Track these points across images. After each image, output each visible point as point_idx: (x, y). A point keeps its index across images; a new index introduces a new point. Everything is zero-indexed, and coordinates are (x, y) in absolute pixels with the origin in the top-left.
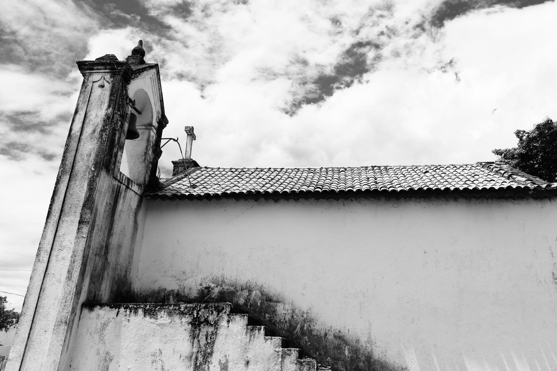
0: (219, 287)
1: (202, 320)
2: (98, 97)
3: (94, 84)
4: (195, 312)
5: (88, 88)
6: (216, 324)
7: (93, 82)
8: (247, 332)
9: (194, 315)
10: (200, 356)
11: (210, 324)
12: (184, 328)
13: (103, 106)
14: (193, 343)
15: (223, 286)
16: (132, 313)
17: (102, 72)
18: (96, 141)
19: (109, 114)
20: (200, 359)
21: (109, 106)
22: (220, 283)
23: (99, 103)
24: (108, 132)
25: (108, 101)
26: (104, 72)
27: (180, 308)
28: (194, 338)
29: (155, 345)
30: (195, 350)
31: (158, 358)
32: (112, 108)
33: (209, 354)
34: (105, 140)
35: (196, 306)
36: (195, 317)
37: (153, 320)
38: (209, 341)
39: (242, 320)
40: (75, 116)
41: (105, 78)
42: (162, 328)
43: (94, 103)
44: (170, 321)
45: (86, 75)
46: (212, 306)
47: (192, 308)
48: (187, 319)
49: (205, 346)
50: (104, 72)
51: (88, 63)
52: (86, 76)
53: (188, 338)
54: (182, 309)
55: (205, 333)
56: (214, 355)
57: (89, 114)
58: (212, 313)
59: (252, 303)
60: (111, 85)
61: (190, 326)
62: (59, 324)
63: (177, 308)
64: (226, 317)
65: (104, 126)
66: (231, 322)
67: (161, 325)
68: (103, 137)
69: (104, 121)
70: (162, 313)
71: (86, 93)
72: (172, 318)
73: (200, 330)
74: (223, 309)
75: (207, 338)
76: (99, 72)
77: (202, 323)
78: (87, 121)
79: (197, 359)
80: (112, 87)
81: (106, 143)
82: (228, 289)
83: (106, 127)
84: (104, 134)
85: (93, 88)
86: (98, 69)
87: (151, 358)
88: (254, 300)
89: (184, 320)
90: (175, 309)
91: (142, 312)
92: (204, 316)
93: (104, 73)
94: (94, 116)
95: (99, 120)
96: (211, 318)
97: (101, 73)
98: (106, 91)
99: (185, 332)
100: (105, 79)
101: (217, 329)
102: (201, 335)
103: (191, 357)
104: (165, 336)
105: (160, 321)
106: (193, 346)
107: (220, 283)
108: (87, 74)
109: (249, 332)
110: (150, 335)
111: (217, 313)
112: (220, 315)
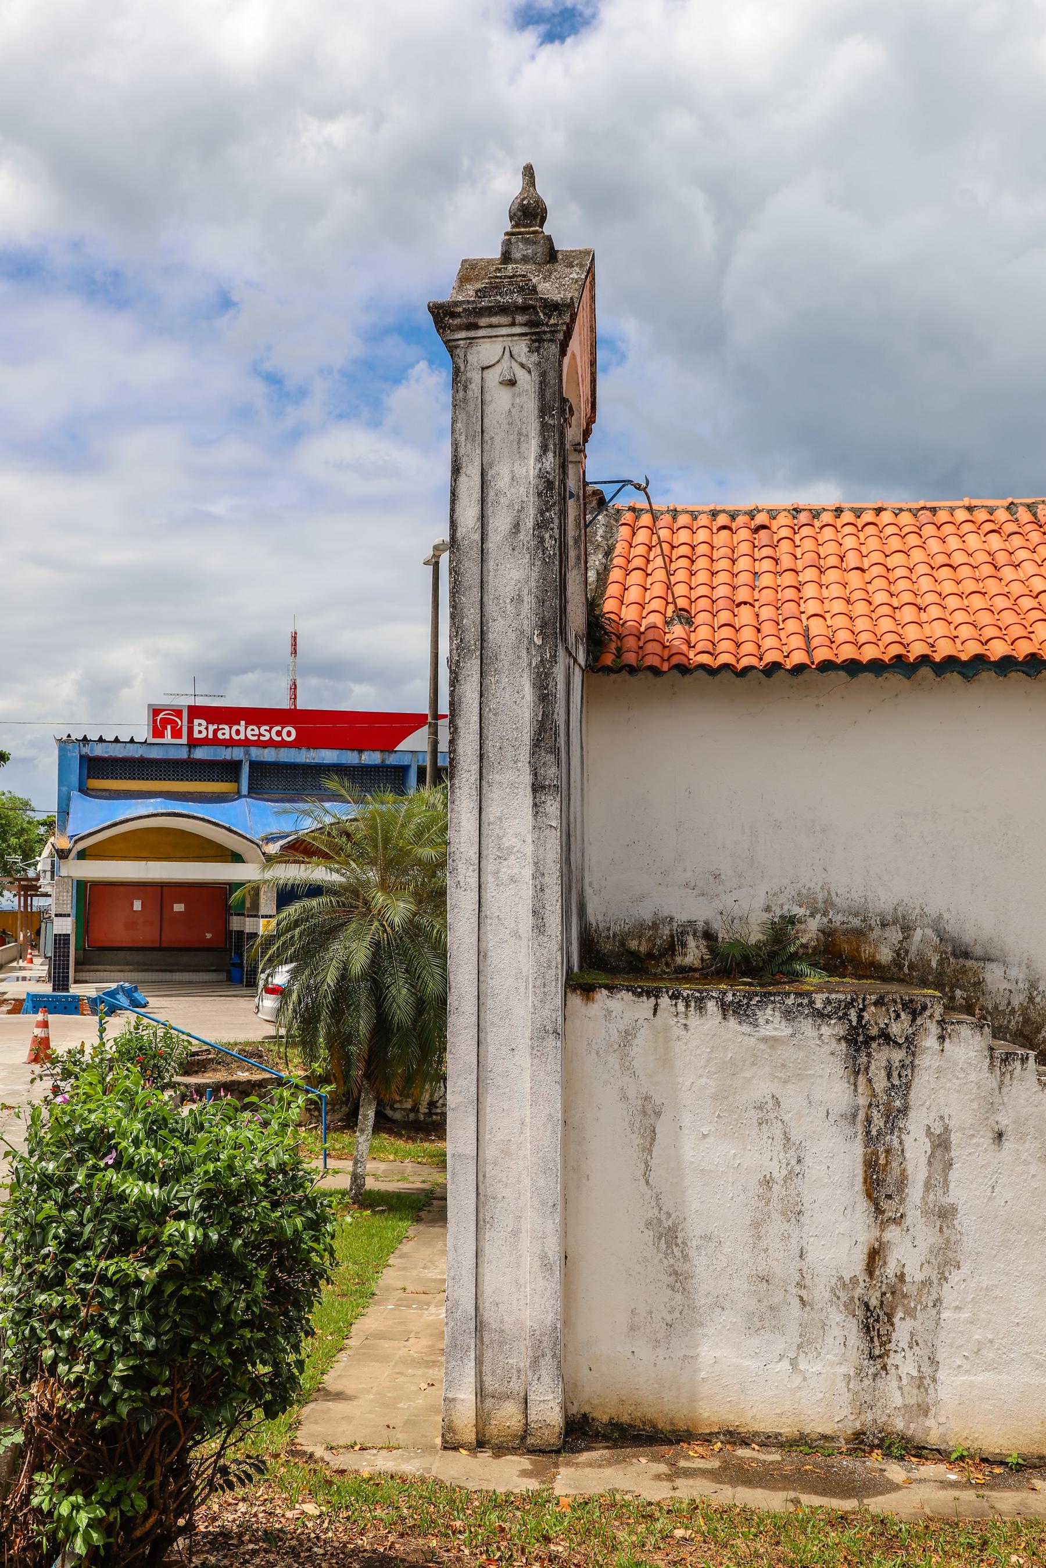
0: (818, 917)
1: (874, 1031)
2: (503, 416)
3: (486, 372)
4: (853, 1015)
5: (473, 391)
6: (910, 1043)
7: (483, 369)
8: (992, 1065)
9: (850, 1021)
10: (875, 1114)
11: (896, 1043)
12: (827, 1049)
13: (524, 445)
14: (855, 1085)
15: (831, 914)
16: (692, 1009)
17: (503, 336)
18: (528, 556)
19: (547, 472)
20: (878, 1122)
21: (544, 448)
22: (820, 905)
23: (511, 437)
24: (556, 531)
25: (537, 432)
26: (508, 336)
27: (812, 1003)
28: (857, 1073)
29: (763, 1088)
30: (863, 1101)
31: (772, 1116)
32: (555, 452)
33: (899, 1111)
34: (555, 554)
35: (853, 1000)
36: (854, 1024)
37: (746, 1028)
38: (896, 1082)
39: (978, 1037)
40: (455, 480)
41: (514, 353)
42: (772, 1047)
43: (497, 439)
44: (790, 1031)
45: (457, 347)
46: (895, 1002)
47: (843, 1004)
48: (832, 1029)
49: (887, 1092)
50: (508, 336)
51: (460, 309)
52: (458, 350)
53: (841, 1073)
54: (819, 1005)
55: (884, 1064)
56: (912, 1114)
57: (491, 473)
58: (898, 1016)
59: (913, 959)
60: (535, 374)
61: (844, 1045)
62: (541, 1034)
63: (806, 1001)
64: (934, 1029)
65: (542, 513)
66: (947, 1040)
67: (772, 1041)
68: (547, 545)
69: (539, 495)
70: (769, 1011)
71: (471, 407)
72: (796, 1024)
73: (869, 1055)
74: (924, 1008)
75: (889, 1076)
76: (494, 334)
77: (873, 1039)
78: (491, 496)
79: (869, 1120)
80: (541, 383)
81: (557, 563)
82: (843, 923)
83: (548, 514)
84: (547, 536)
85: (486, 389)
86: (491, 326)
87: (755, 1115)
88: (920, 954)
89: (826, 1030)
90: (800, 1005)
91: (716, 1009)
92: (877, 1024)
93: (510, 339)
94: (507, 479)
95: (522, 490)
96: (895, 1029)
97: (501, 339)
98: (524, 398)
99: (831, 1058)
100: (516, 356)
101: (914, 1054)
102: (872, 1067)
103: (854, 1116)
104: (783, 1065)
105: (766, 1031)
106: (856, 1090)
107: (820, 905)
108: (461, 342)
109: (999, 1065)
110: (744, 1061)
111: (910, 1017)
112: (919, 1022)
